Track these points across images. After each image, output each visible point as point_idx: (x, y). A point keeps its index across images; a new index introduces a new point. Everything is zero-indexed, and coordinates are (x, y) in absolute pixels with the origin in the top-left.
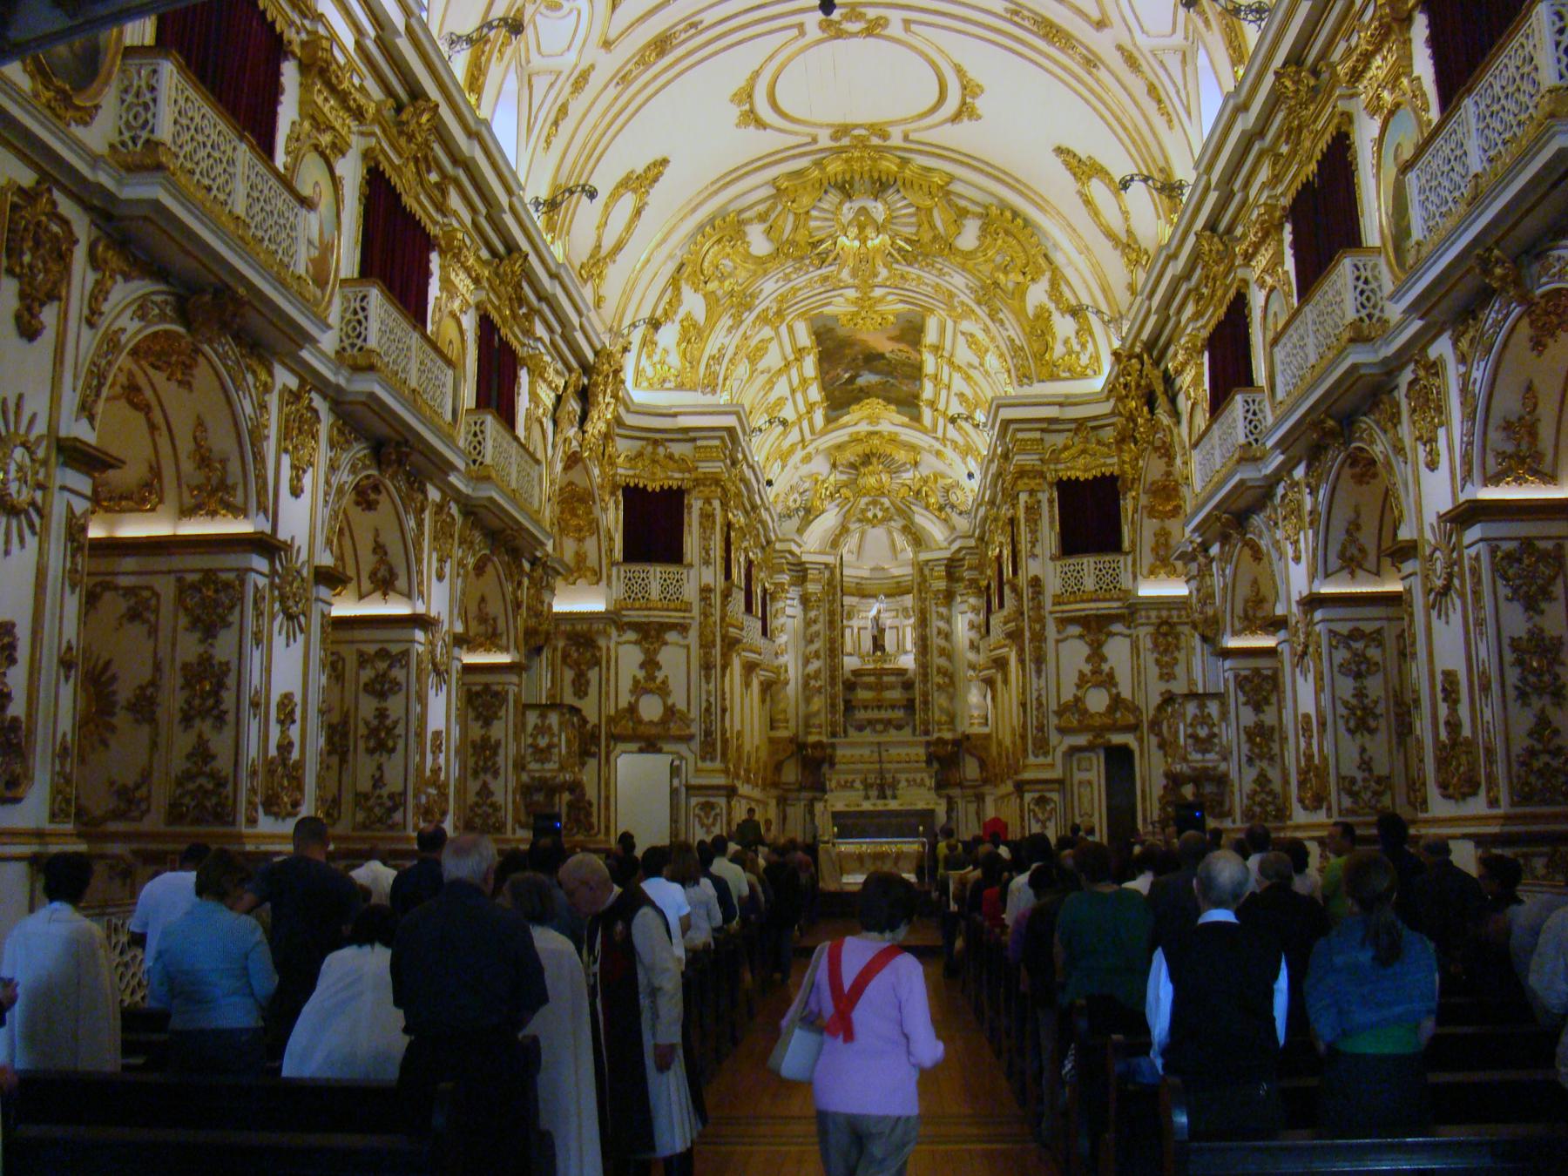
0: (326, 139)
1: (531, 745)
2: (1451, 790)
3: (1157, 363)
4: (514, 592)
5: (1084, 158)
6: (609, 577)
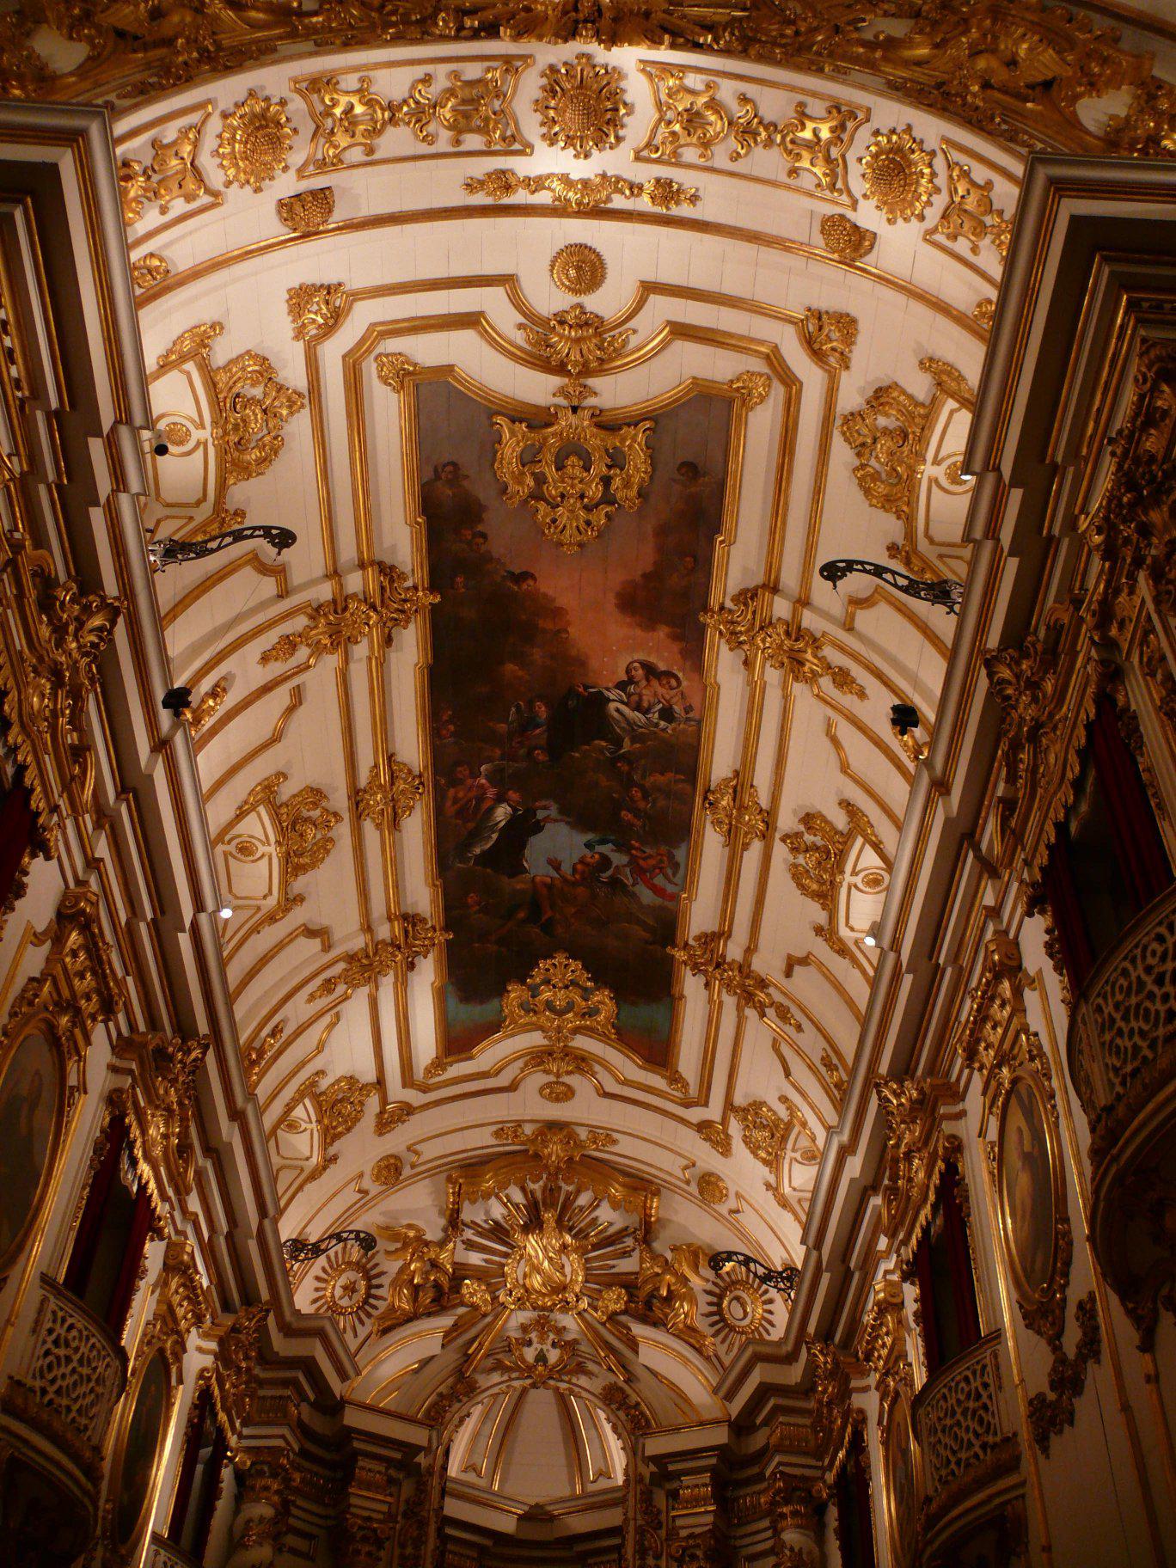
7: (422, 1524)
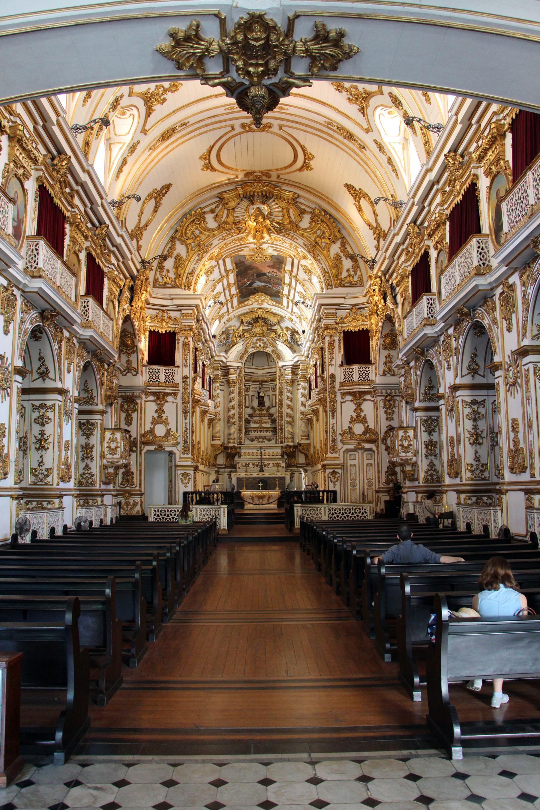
0: (21, 171)
1: (107, 447)
2: (514, 470)
3: (388, 281)
4: (101, 378)
5: (358, 189)
6: (142, 371)
7: (241, 377)
